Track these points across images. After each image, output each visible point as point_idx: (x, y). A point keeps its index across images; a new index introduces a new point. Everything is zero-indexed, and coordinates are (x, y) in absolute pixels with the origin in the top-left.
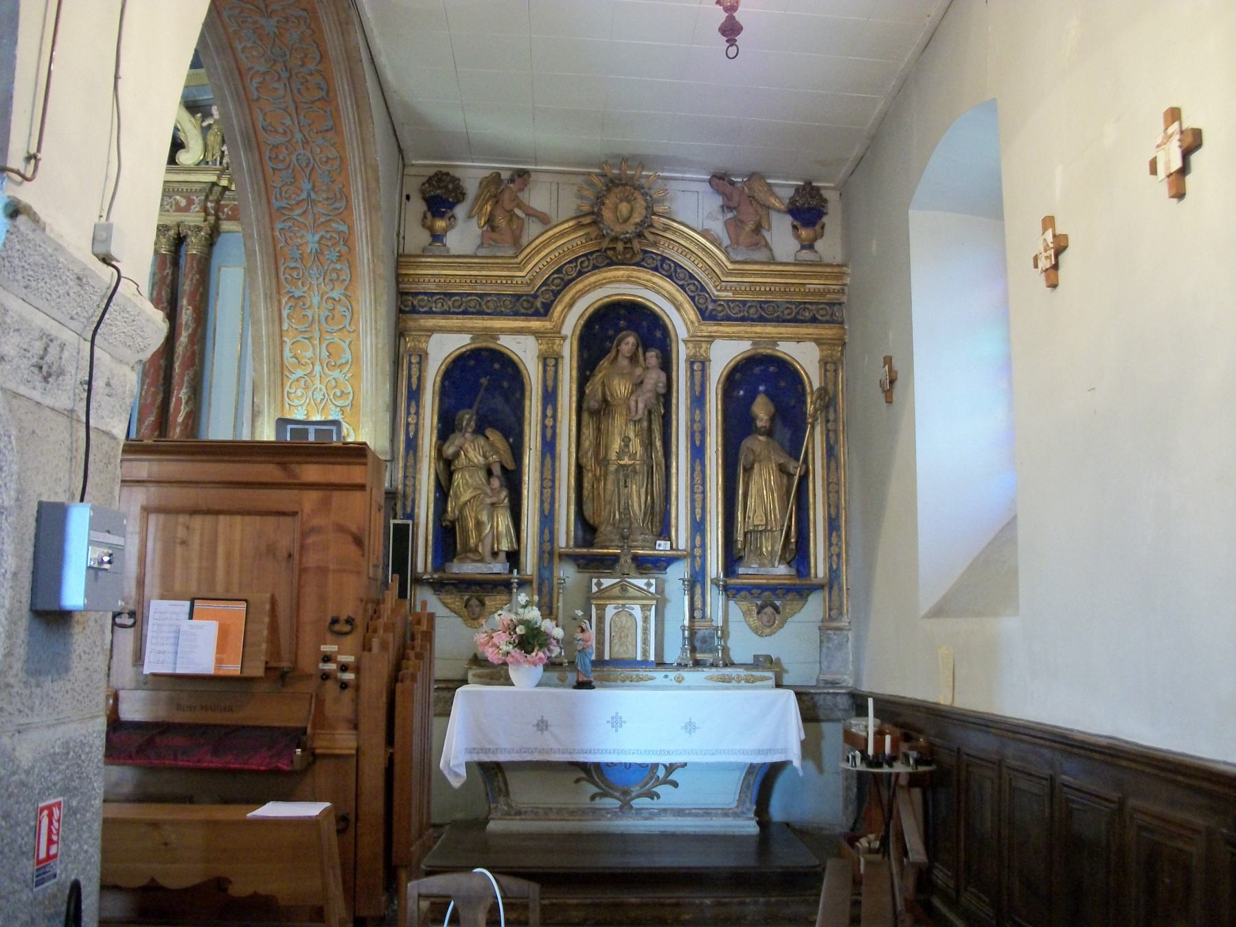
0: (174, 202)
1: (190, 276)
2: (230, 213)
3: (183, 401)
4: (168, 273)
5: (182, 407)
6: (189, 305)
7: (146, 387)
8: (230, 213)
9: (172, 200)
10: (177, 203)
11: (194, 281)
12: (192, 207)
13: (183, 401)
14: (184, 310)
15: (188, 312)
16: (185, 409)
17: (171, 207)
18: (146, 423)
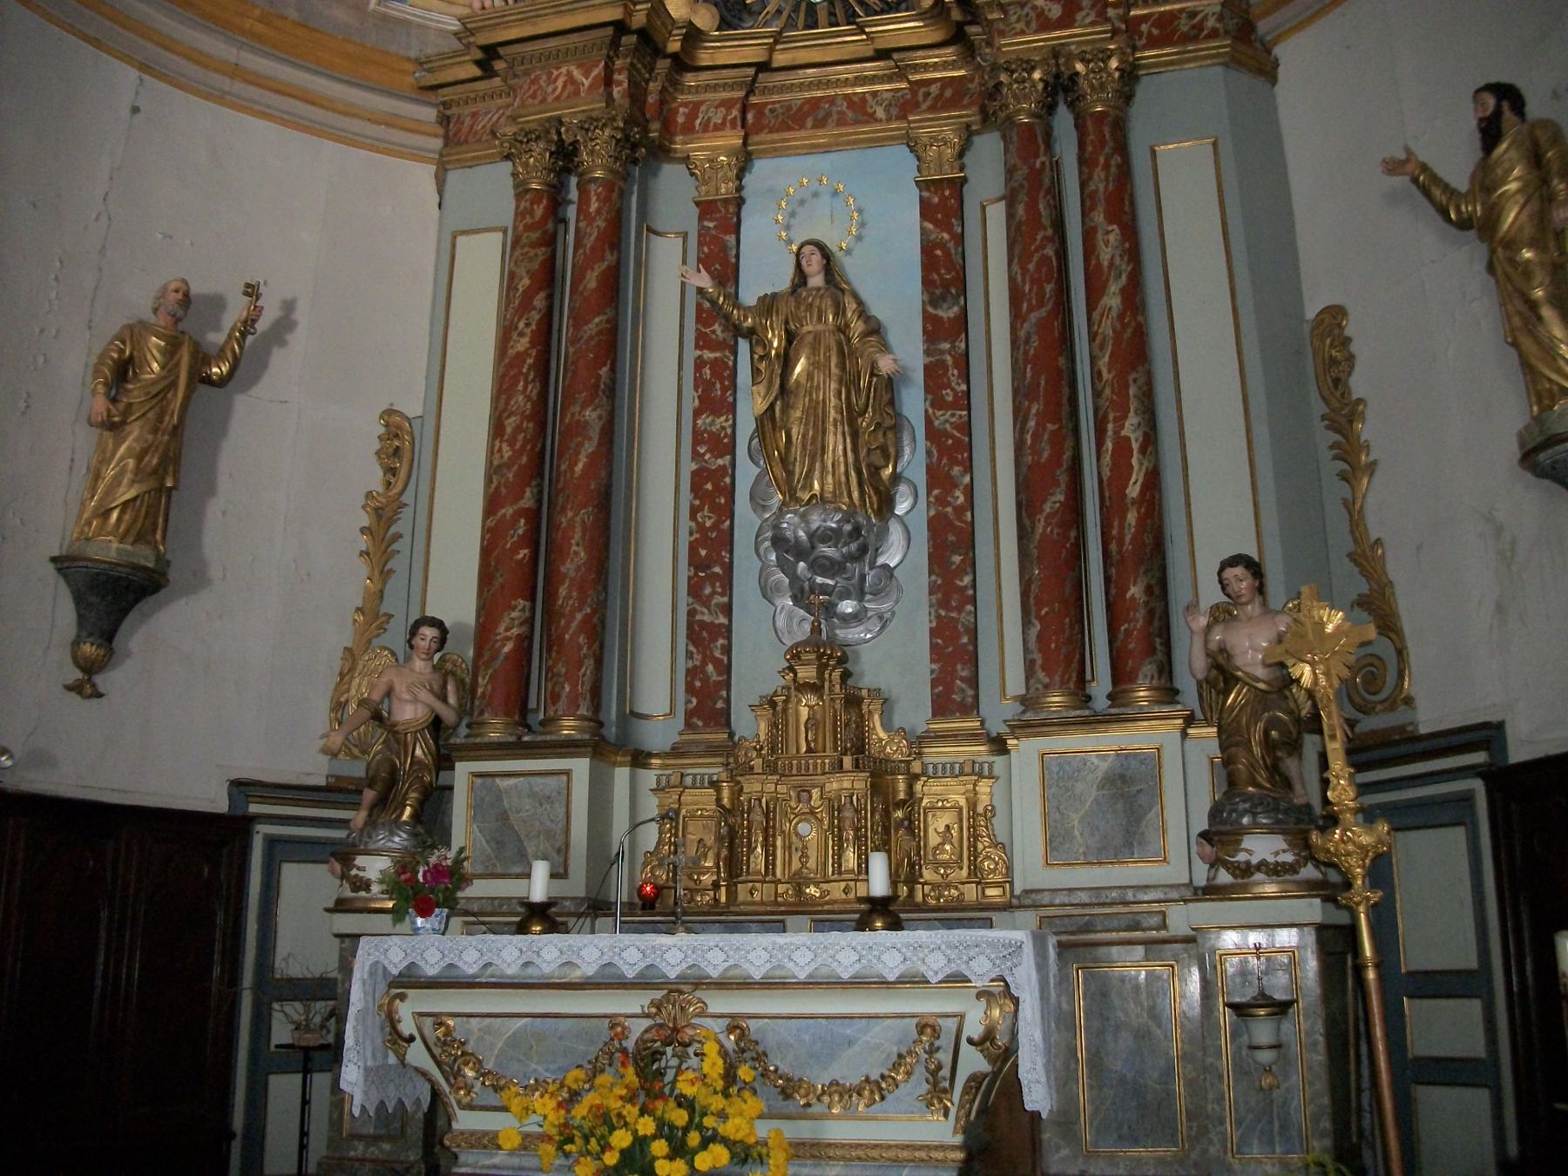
0: (1033, 14)
1: (1102, 160)
2: (1155, 32)
3: (1135, 446)
4: (1043, 164)
5: (1134, 461)
6: (1111, 222)
7: (1032, 423)
8: (1155, 32)
9: (1026, 10)
10: (1041, 14)
11: (1113, 169)
12: (1079, 16)
13: (1135, 446)
14: (1099, 236)
15: (1112, 237)
16: (1141, 464)
17: (1028, 24)
18: (1047, 508)
